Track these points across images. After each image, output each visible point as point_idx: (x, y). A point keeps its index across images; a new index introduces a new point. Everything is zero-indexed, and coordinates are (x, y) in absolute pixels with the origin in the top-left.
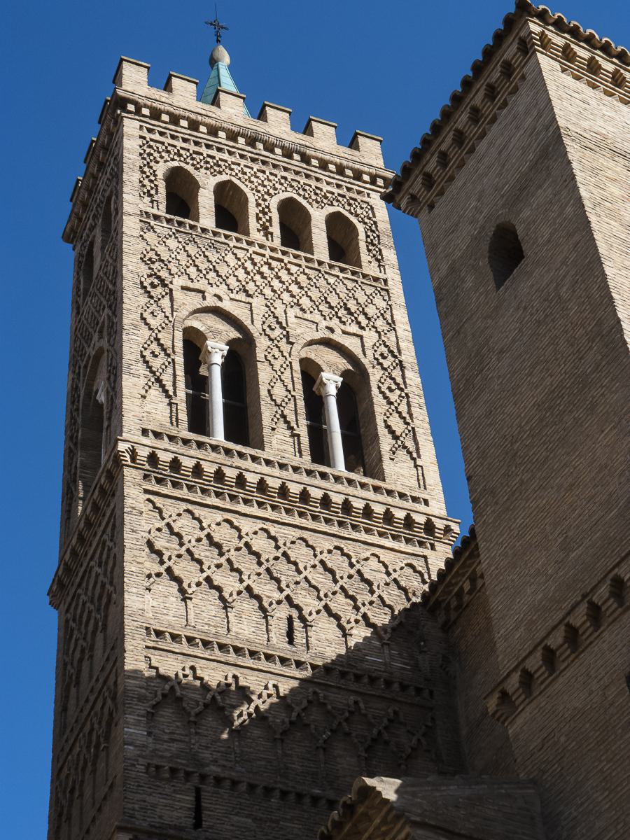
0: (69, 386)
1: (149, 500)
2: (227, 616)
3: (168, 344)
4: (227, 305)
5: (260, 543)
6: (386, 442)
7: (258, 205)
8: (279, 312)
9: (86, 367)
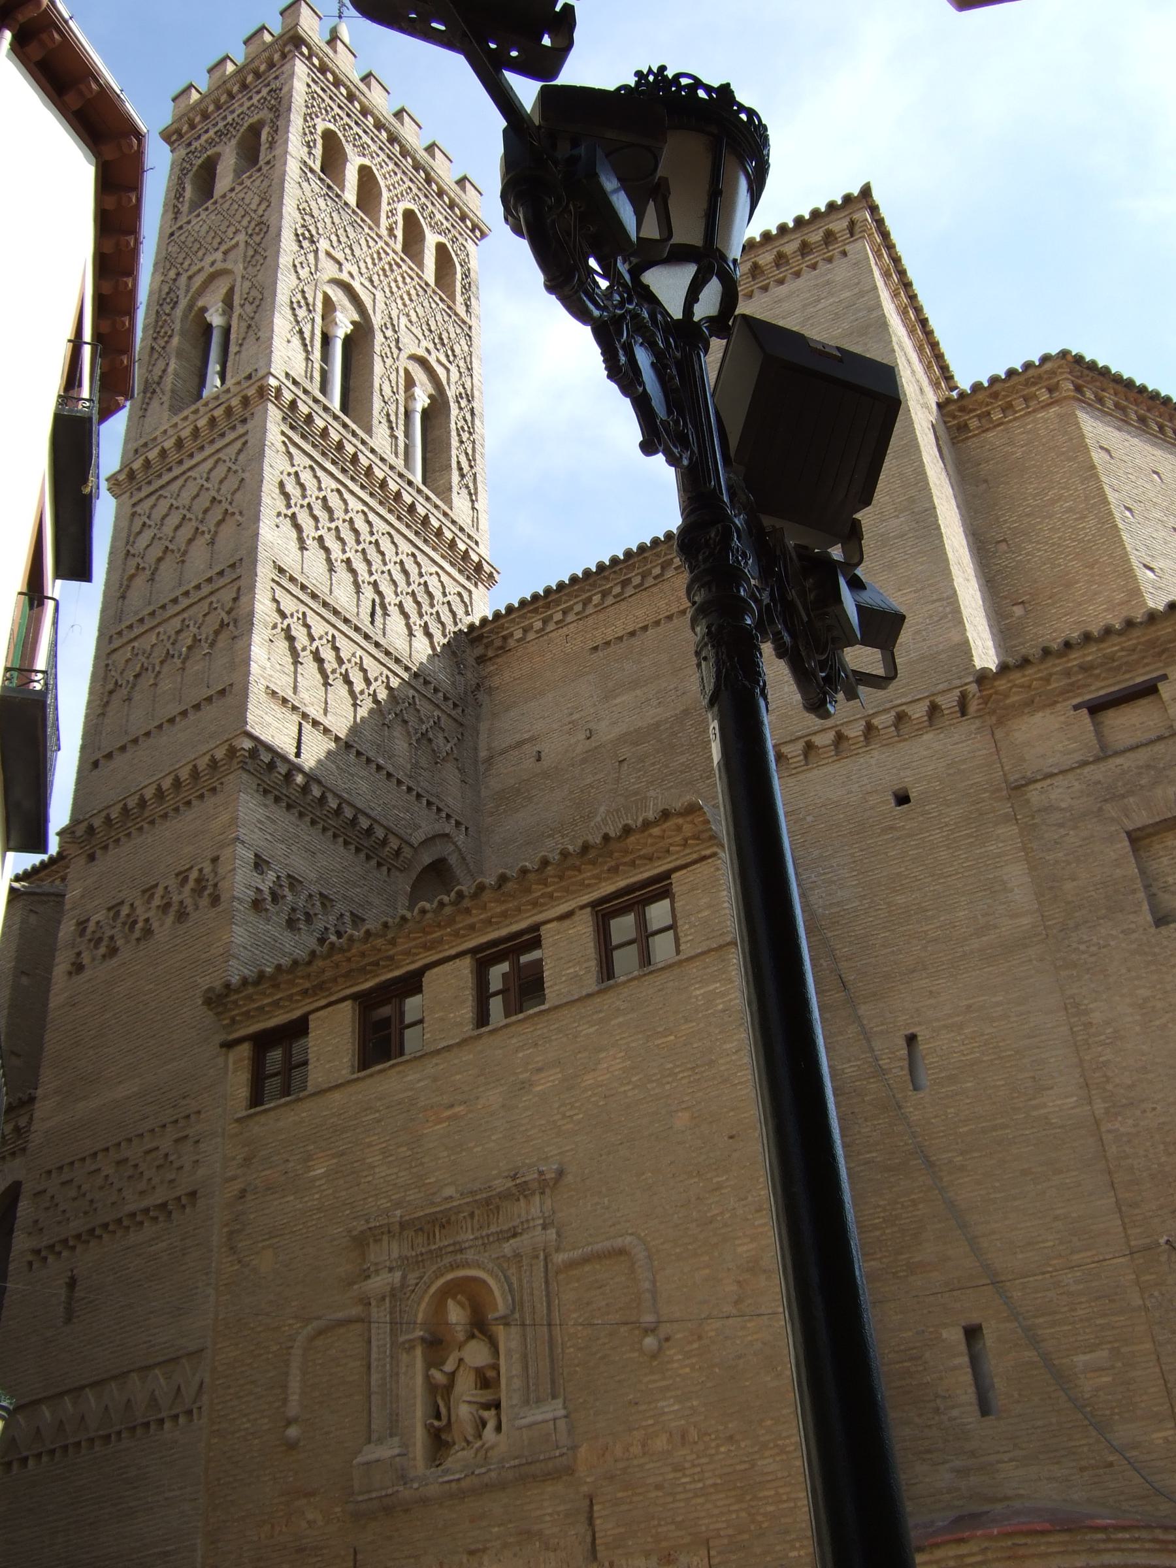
0: (156, 287)
1: (284, 442)
2: (331, 579)
3: (310, 300)
4: (356, 285)
5: (360, 524)
6: (455, 477)
7: (389, 204)
8: (394, 314)
9: (190, 278)
